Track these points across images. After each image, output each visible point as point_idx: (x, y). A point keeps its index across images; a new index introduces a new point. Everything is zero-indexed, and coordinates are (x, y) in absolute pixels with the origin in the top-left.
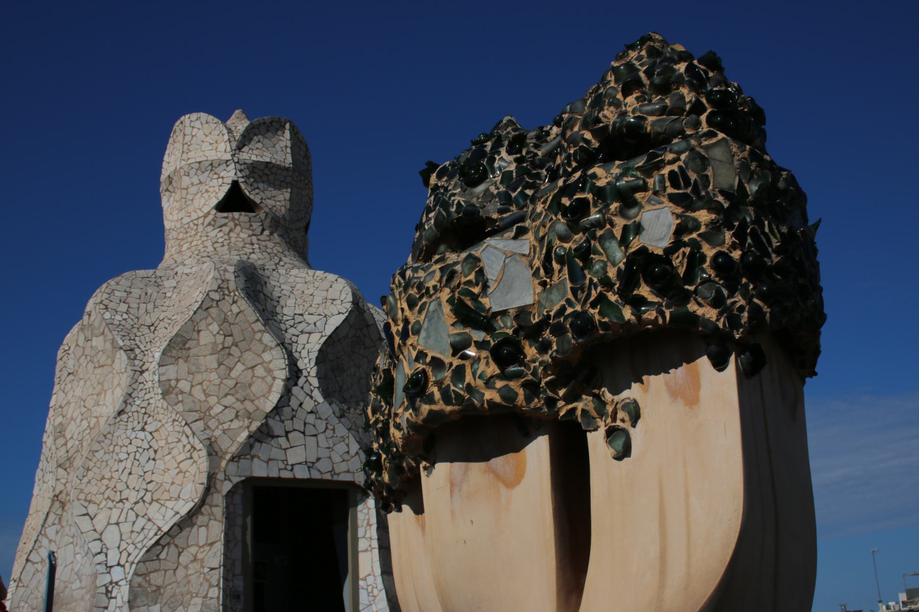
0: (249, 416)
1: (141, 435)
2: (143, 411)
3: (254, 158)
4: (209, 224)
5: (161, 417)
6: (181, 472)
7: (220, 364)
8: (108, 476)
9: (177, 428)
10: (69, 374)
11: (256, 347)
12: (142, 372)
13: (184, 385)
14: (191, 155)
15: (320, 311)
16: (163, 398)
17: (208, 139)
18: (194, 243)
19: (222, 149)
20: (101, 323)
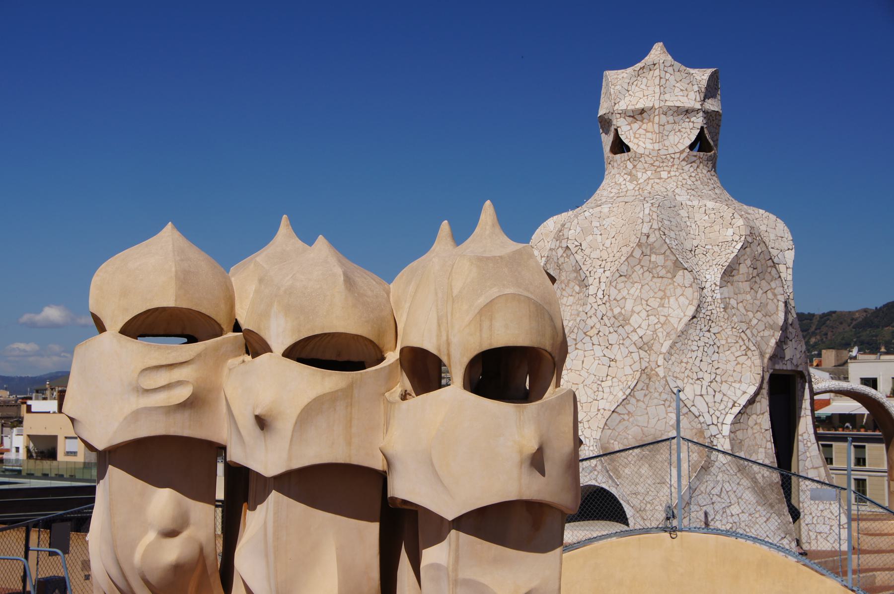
0: (771, 327)
1: (707, 334)
2: (708, 318)
3: (712, 108)
4: (684, 160)
5: (722, 324)
6: (738, 363)
7: (752, 289)
8: (685, 360)
9: (736, 334)
10: (621, 276)
11: (768, 277)
12: (703, 289)
13: (733, 302)
14: (667, 97)
15: (777, 246)
16: (725, 311)
17: (678, 85)
18: (673, 174)
19: (692, 100)
20: (662, 246)
